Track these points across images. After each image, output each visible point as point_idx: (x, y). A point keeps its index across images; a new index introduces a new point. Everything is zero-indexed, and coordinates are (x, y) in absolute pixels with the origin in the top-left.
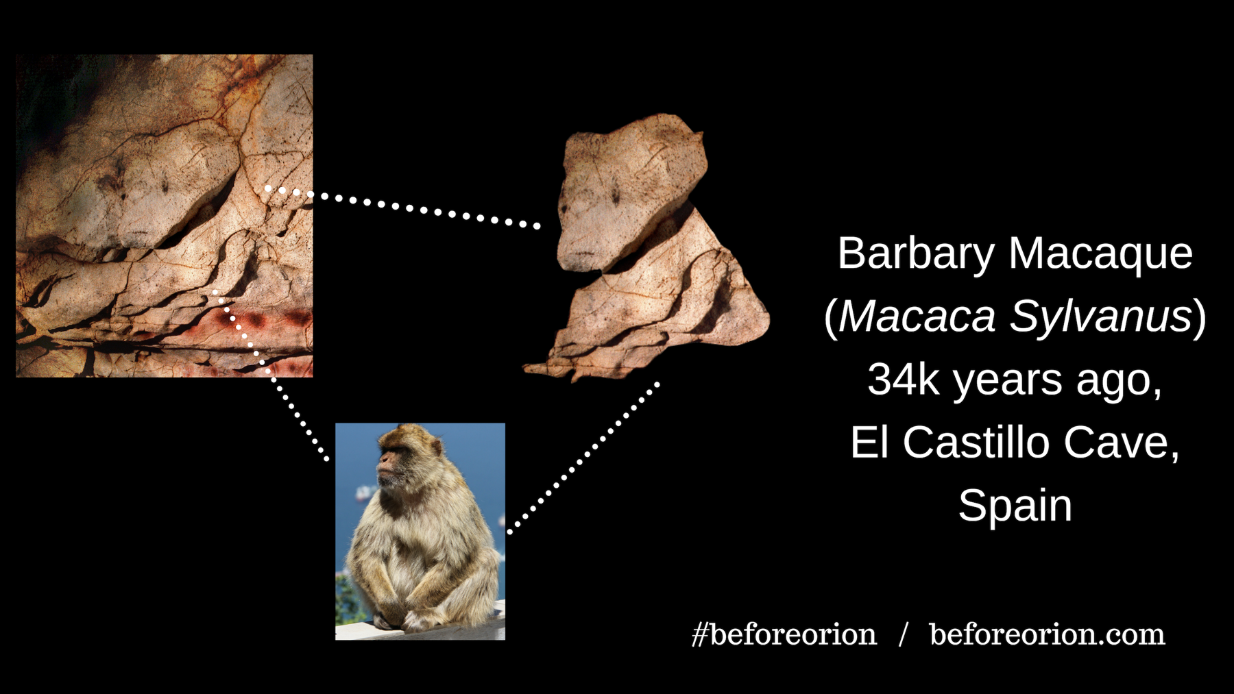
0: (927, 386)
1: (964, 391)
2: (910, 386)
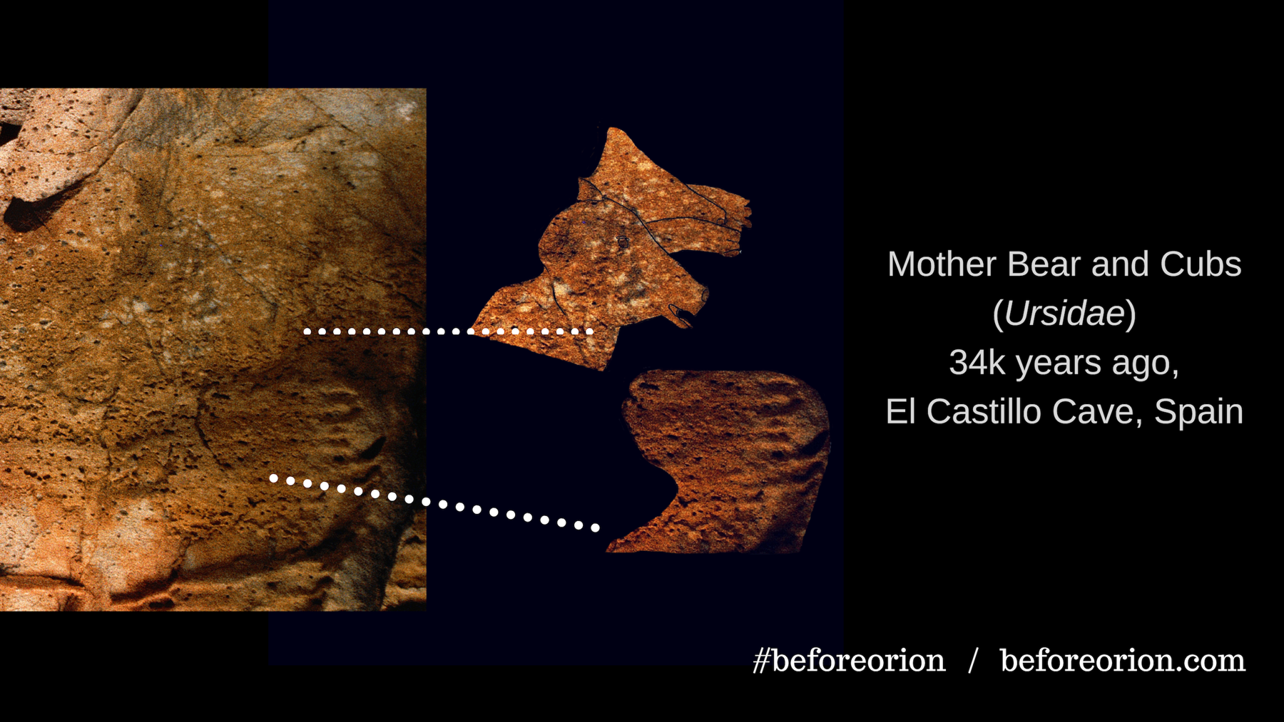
0: (995, 368)
2: (982, 368)
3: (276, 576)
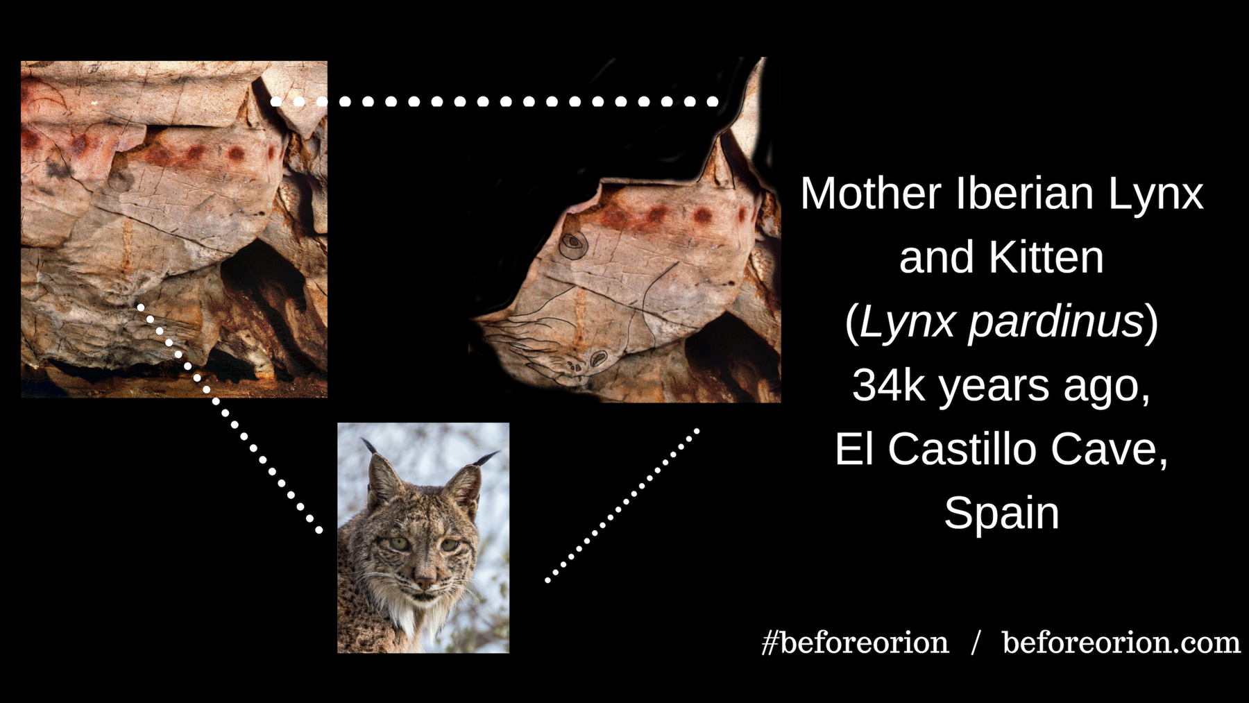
0: (912, 393)
1: (950, 397)
2: (895, 392)
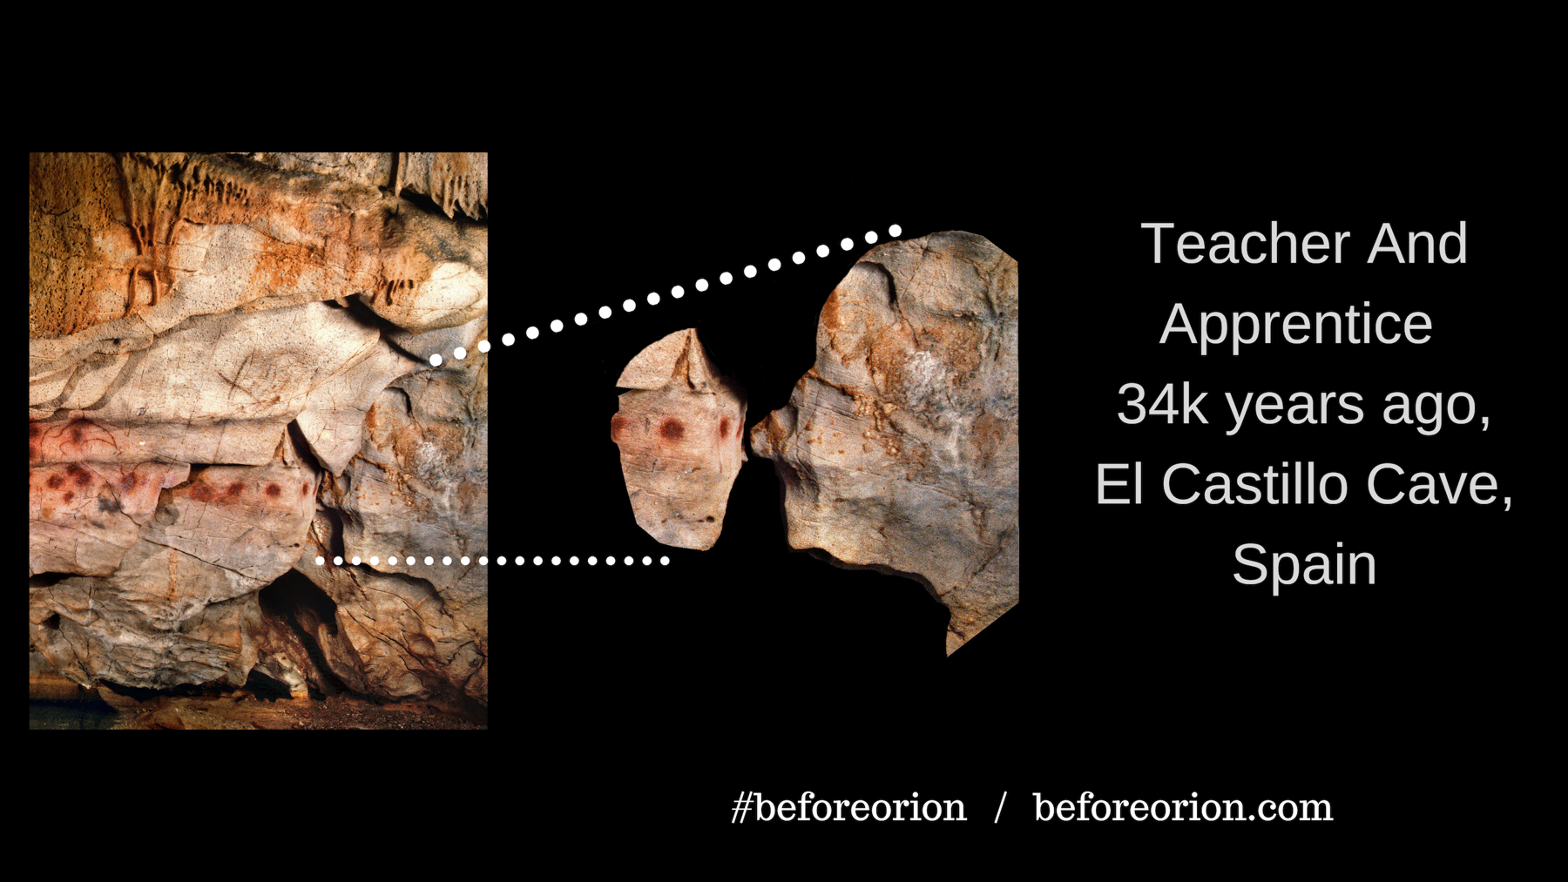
3: (129, 178)
